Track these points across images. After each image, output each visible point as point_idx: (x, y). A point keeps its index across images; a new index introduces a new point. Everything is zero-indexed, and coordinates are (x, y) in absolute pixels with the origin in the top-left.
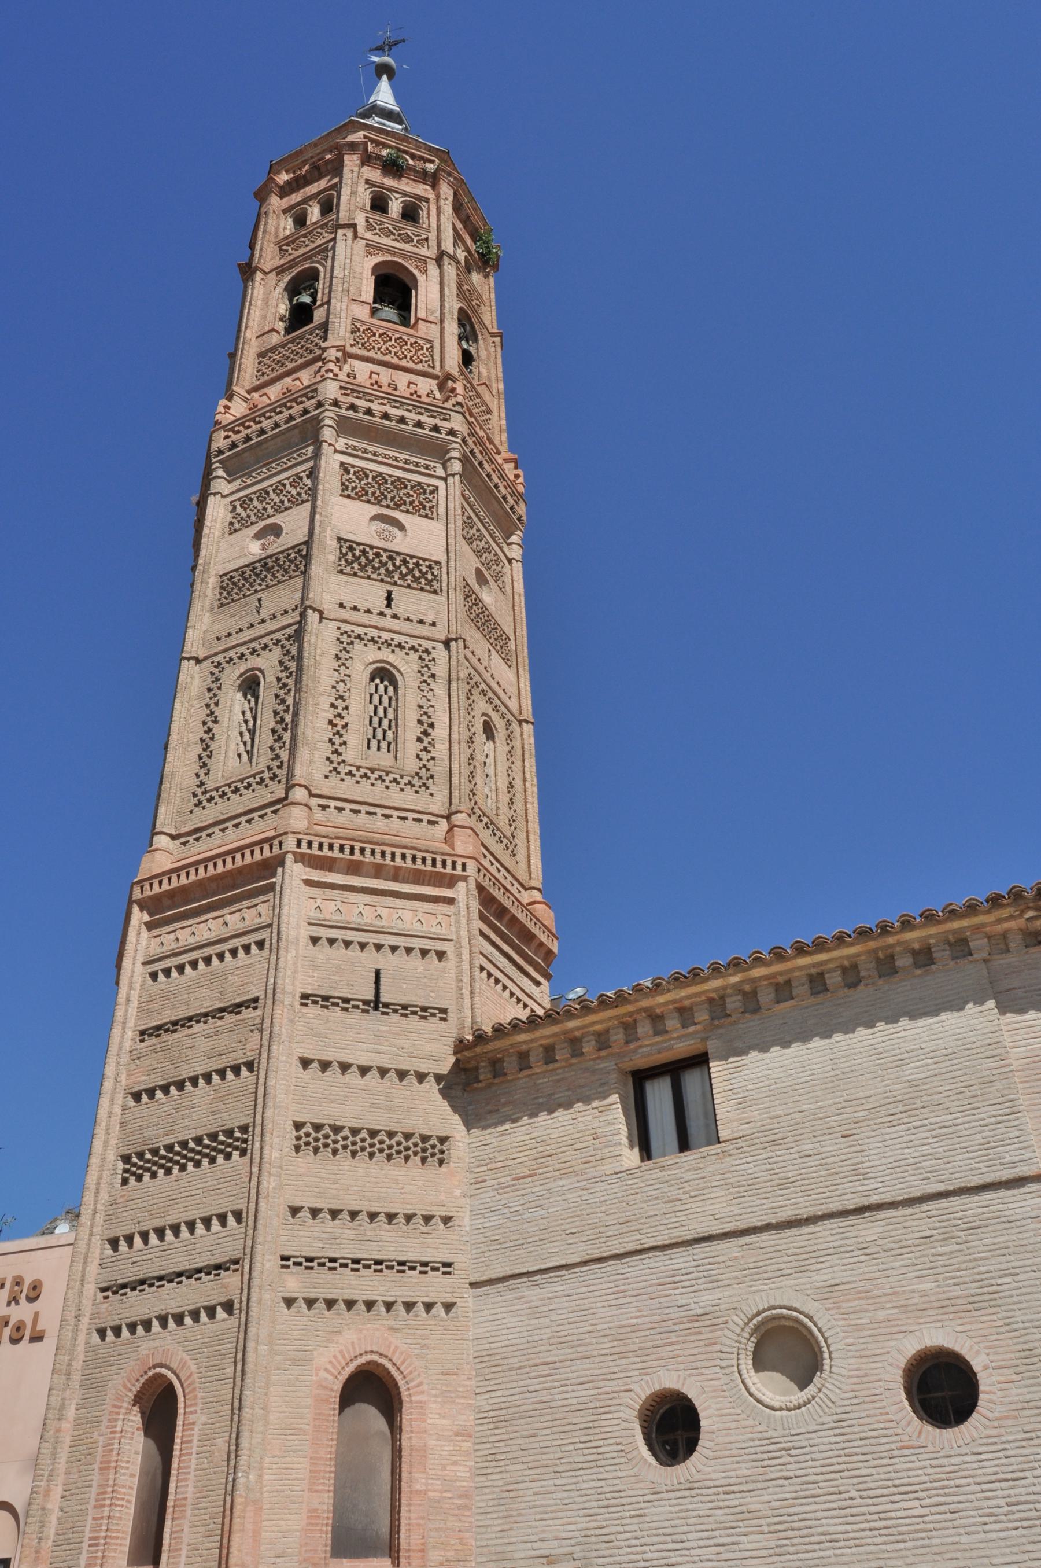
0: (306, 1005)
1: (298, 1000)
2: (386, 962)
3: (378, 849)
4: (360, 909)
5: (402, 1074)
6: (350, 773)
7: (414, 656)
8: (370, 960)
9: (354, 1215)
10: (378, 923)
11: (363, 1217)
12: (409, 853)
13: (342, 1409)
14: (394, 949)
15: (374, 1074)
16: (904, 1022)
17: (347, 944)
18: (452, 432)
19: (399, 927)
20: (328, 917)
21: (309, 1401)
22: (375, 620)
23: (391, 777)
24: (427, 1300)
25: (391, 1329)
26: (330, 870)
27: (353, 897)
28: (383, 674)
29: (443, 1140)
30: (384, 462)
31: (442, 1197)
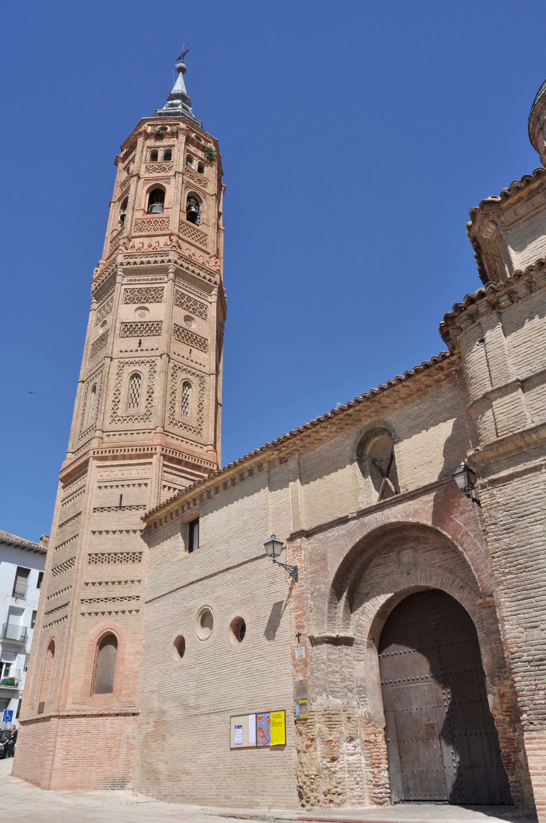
0: (95, 512)
1: (92, 510)
2: (124, 491)
3: (123, 449)
4: (117, 473)
5: (128, 532)
6: (119, 420)
8: (117, 492)
9: (107, 583)
10: (123, 477)
11: (110, 583)
12: (134, 448)
13: (100, 648)
14: (128, 485)
15: (118, 533)
16: (246, 498)
17: (111, 487)
18: (169, 261)
19: (131, 477)
20: (104, 478)
21: (87, 646)
22: (134, 354)
23: (135, 417)
24: (129, 609)
25: (116, 620)
26: (107, 460)
27: (114, 469)
28: (136, 376)
29: (141, 553)
30: (143, 283)
31: (138, 574)
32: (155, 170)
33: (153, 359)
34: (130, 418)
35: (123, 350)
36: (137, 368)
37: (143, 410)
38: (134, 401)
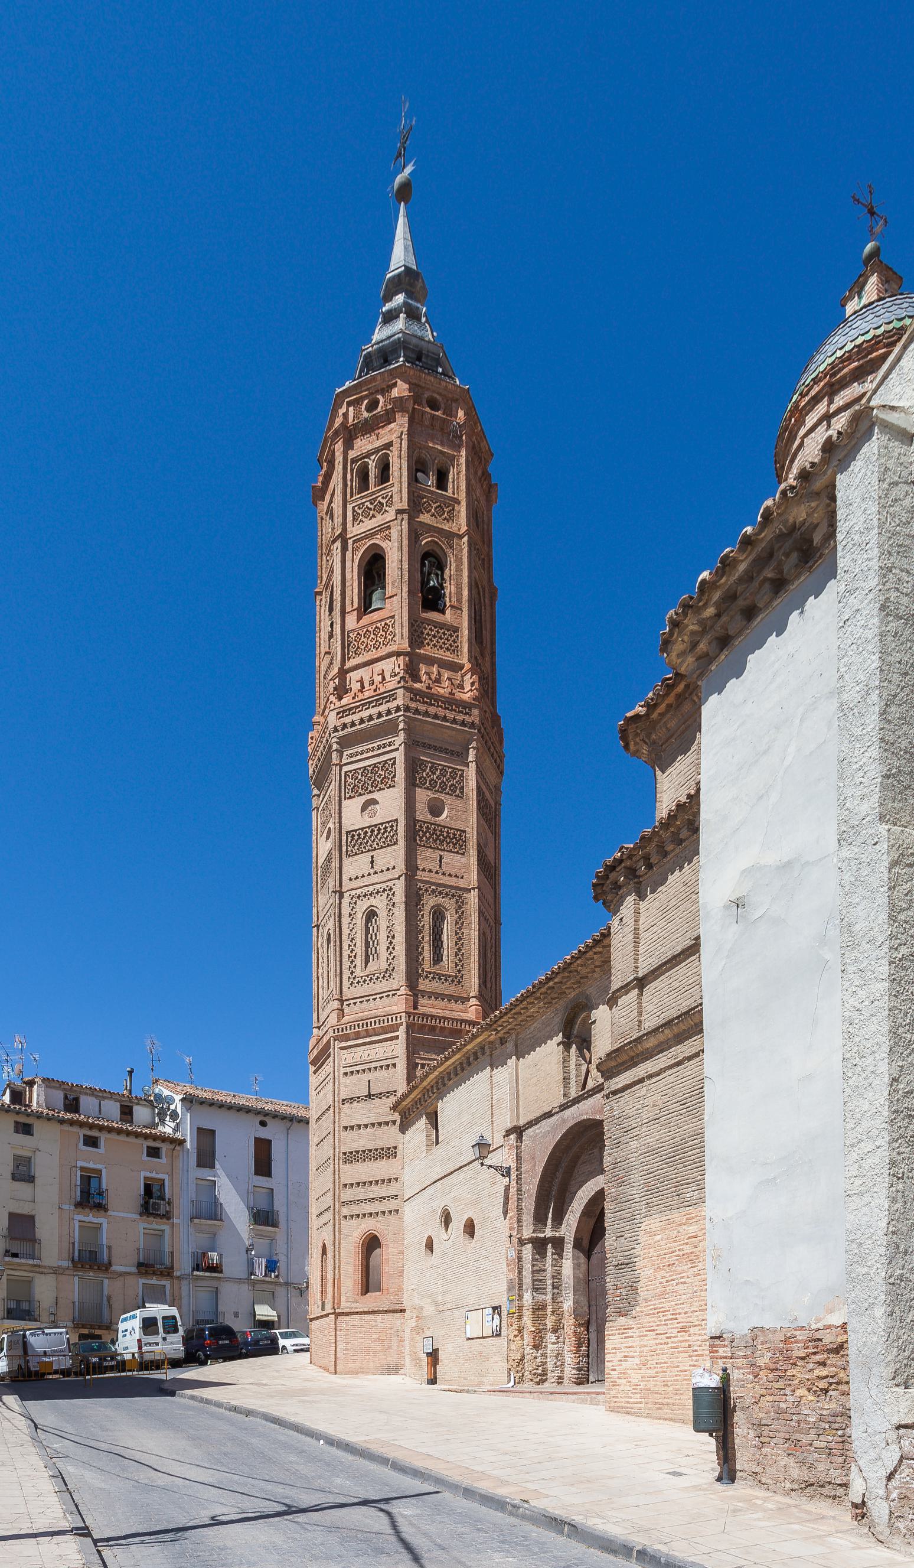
2: (371, 1076)
5: (380, 1124)
8: (365, 1077)
22: (367, 881)
29: (395, 1148)
34: (371, 978)
35: (353, 877)
36: (373, 901)
37: (384, 965)
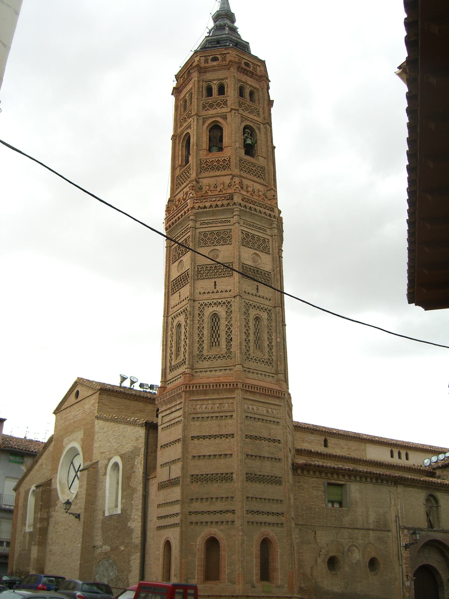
7: (224, 306)
32: (211, 106)
33: (229, 300)
38: (216, 340)
